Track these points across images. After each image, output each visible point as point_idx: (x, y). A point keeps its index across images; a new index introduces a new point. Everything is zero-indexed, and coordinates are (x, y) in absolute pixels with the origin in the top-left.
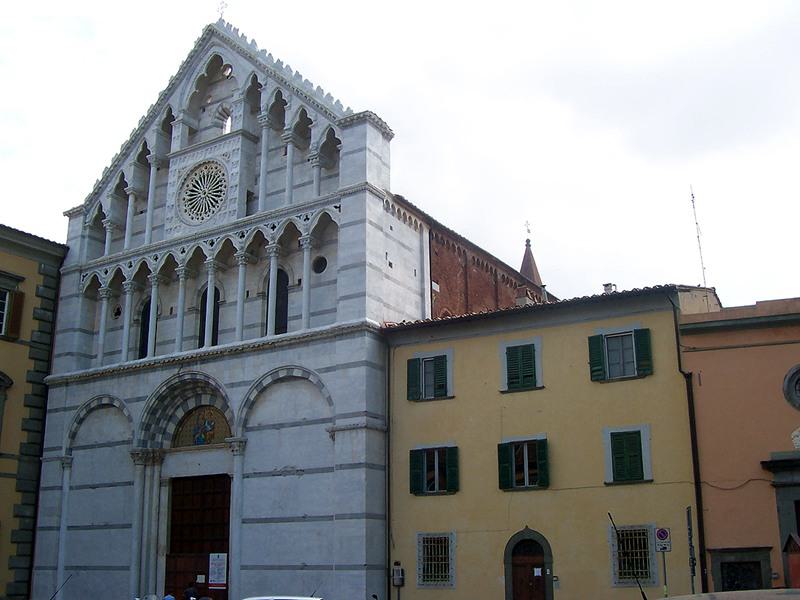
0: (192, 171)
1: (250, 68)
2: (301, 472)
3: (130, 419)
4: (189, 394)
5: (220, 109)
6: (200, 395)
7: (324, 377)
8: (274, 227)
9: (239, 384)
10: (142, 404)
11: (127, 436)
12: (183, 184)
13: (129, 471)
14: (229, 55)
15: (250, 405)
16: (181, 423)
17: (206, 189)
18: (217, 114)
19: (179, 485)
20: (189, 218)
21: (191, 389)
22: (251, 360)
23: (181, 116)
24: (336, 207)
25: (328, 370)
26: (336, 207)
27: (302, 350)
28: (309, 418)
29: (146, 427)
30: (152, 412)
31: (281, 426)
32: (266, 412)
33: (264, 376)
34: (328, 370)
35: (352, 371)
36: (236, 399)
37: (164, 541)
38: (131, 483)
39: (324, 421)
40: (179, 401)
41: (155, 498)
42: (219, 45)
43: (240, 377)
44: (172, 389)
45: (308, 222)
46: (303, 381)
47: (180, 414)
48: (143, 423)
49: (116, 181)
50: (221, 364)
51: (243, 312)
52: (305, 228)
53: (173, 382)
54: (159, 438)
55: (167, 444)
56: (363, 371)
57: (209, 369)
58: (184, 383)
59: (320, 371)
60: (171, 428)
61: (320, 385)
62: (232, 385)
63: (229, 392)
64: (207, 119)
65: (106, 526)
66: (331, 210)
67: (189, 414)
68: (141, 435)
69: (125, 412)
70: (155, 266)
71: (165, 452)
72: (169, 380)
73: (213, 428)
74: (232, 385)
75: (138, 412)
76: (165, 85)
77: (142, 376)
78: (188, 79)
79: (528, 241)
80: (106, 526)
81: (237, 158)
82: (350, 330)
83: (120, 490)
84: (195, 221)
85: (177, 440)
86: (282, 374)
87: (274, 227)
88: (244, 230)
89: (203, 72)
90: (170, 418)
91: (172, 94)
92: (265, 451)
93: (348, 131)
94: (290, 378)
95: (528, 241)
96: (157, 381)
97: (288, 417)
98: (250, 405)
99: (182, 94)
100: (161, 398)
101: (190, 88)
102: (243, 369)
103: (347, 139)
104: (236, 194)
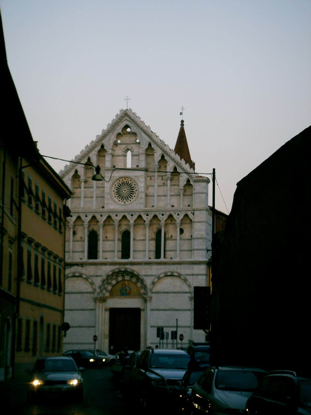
0: (118, 179)
1: (148, 140)
2: (177, 310)
3: (92, 284)
4: (120, 275)
5: (126, 148)
6: (125, 276)
7: (188, 277)
8: (163, 215)
9: (149, 276)
11: (90, 290)
12: (113, 184)
13: (91, 305)
14: (135, 128)
15: (154, 283)
16: (114, 286)
17: (125, 190)
18: (124, 150)
19: (114, 312)
20: (117, 201)
21: (122, 273)
22: (155, 267)
23: (110, 151)
24: (191, 213)
25: (189, 275)
26: (191, 213)
27: (179, 266)
28: (180, 291)
29: (100, 287)
30: (103, 281)
31: (168, 293)
32: (159, 287)
33: (161, 274)
34: (189, 275)
35: (200, 277)
36: (148, 281)
37: (107, 332)
38: (95, 310)
39: (186, 293)
40: (114, 277)
41: (103, 316)
42: (130, 122)
43: (150, 273)
45: (178, 216)
46: (178, 277)
47: (114, 282)
49: (72, 173)
50: (140, 267)
51: (142, 245)
52: (178, 219)
54: (104, 291)
55: (107, 294)
56: (204, 277)
57: (136, 269)
58: (120, 271)
59: (186, 275)
60: (109, 288)
61: (185, 280)
62: (146, 276)
63: (145, 278)
64: (119, 151)
65: (80, 327)
66: (189, 213)
67: (118, 282)
68: (98, 290)
69: (89, 280)
70: (102, 220)
71: (107, 297)
73: (130, 289)
74: (146, 276)
75: (98, 282)
76: (100, 133)
77: (98, 266)
78: (113, 133)
79: (182, 122)
80: (80, 327)
81: (142, 179)
82: (199, 262)
83: (87, 313)
84: (120, 202)
85: (112, 294)
86: (169, 274)
87: (163, 215)
88: (148, 213)
89: (120, 131)
90: (109, 284)
91: (104, 139)
92: (156, 301)
93: (197, 184)
94: (172, 275)
95: (182, 122)
96: (108, 269)
97: (171, 289)
98: (154, 283)
99: (110, 140)
100: (108, 276)
101: (113, 137)
102: (152, 270)
103: (197, 187)
104: (143, 195)
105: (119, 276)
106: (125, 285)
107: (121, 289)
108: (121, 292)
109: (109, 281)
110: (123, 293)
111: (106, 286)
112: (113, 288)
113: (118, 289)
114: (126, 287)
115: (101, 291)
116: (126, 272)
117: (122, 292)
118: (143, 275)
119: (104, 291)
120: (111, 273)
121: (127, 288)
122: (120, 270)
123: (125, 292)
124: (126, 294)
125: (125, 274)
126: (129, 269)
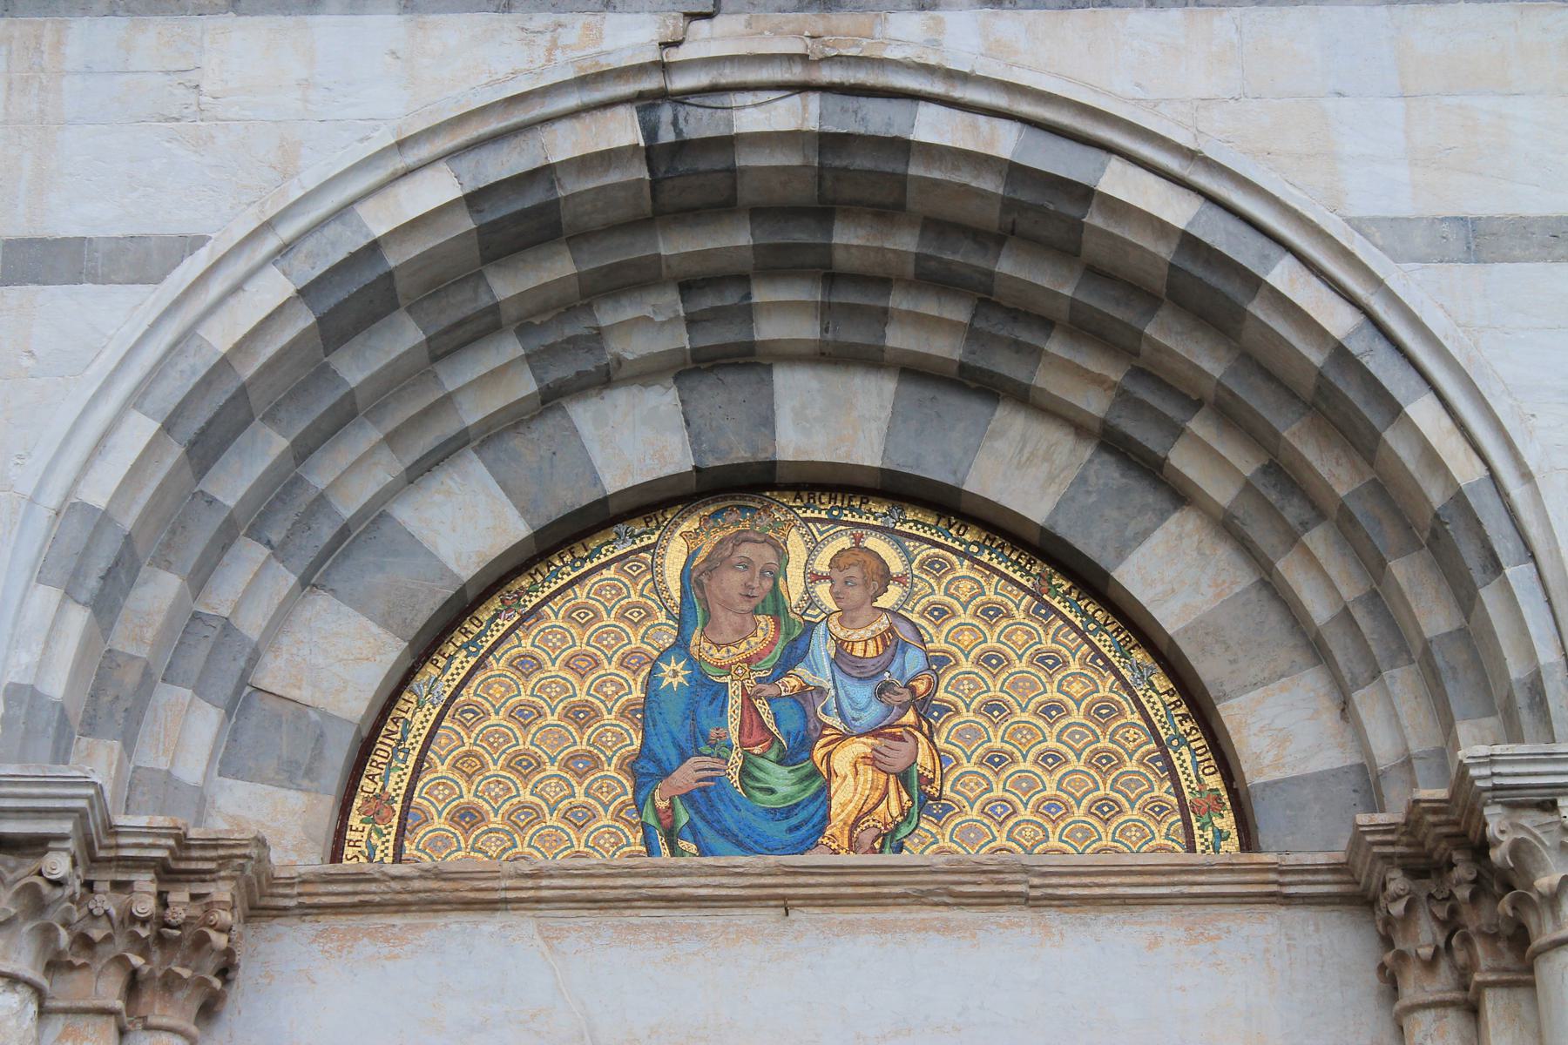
10: (110, 322)
40: (493, 378)
44: (518, 219)
47: (467, 522)
48: (102, 520)
53: (564, 144)
62: (1479, 240)
63: (1431, 294)
72: (519, 116)
74: (1479, 240)
90: (333, 554)
100: (354, 297)
105: (605, 379)
106: (775, 605)
107: (647, 712)
108: (646, 770)
109: (353, 475)
110: (702, 800)
111: (250, 584)
112: (438, 678)
113: (581, 715)
114: (795, 652)
115: (112, 697)
116: (850, 238)
117: (687, 775)
118: (1395, 231)
119: (188, 731)
120: (438, 189)
121: (818, 670)
122: (700, 124)
123: (782, 781)
124: (807, 820)
125: (784, 314)
126: (952, 90)
